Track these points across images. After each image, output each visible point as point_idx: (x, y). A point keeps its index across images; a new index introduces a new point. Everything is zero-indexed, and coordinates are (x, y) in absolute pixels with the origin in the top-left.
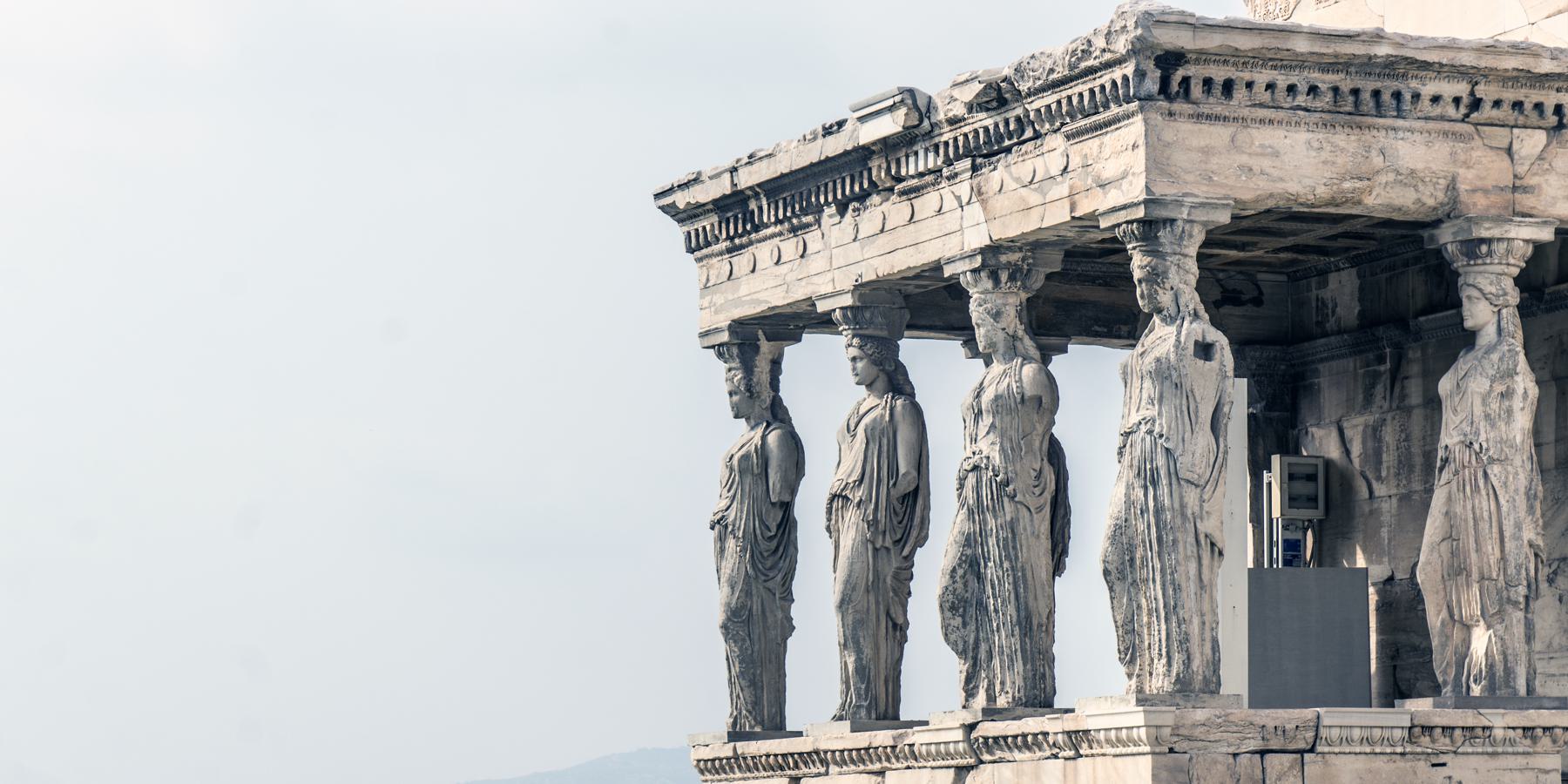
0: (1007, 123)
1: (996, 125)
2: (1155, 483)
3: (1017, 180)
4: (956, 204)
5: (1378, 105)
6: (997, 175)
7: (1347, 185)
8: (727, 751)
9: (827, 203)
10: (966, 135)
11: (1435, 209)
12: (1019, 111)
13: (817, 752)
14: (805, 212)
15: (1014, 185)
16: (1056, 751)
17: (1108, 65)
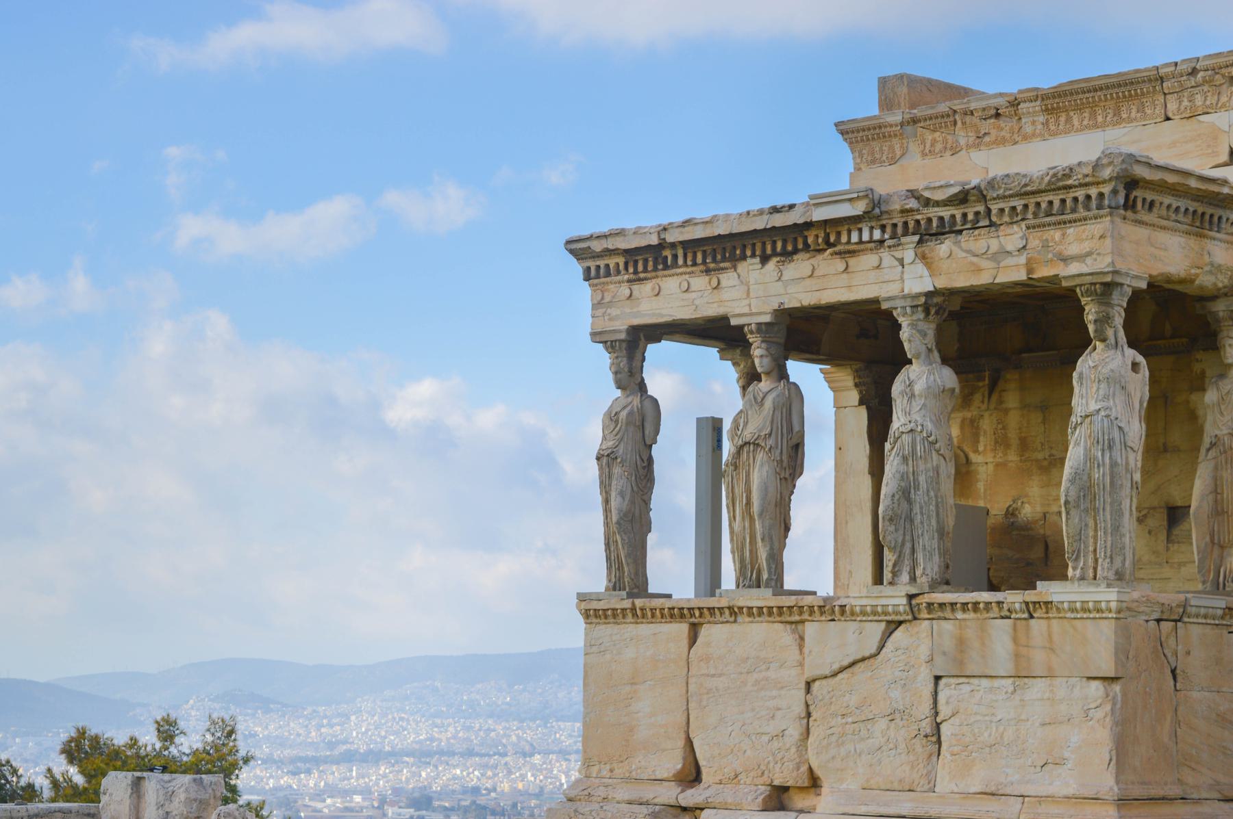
0: (965, 215)
1: (953, 216)
2: (1110, 447)
3: (968, 251)
4: (897, 263)
5: (1211, 222)
6: (944, 247)
7: (1193, 271)
8: (627, 604)
9: (753, 255)
10: (918, 222)
11: (1219, 289)
12: (981, 208)
13: (729, 608)
14: (724, 259)
15: (964, 255)
16: (1005, 613)
17: (1086, 185)
